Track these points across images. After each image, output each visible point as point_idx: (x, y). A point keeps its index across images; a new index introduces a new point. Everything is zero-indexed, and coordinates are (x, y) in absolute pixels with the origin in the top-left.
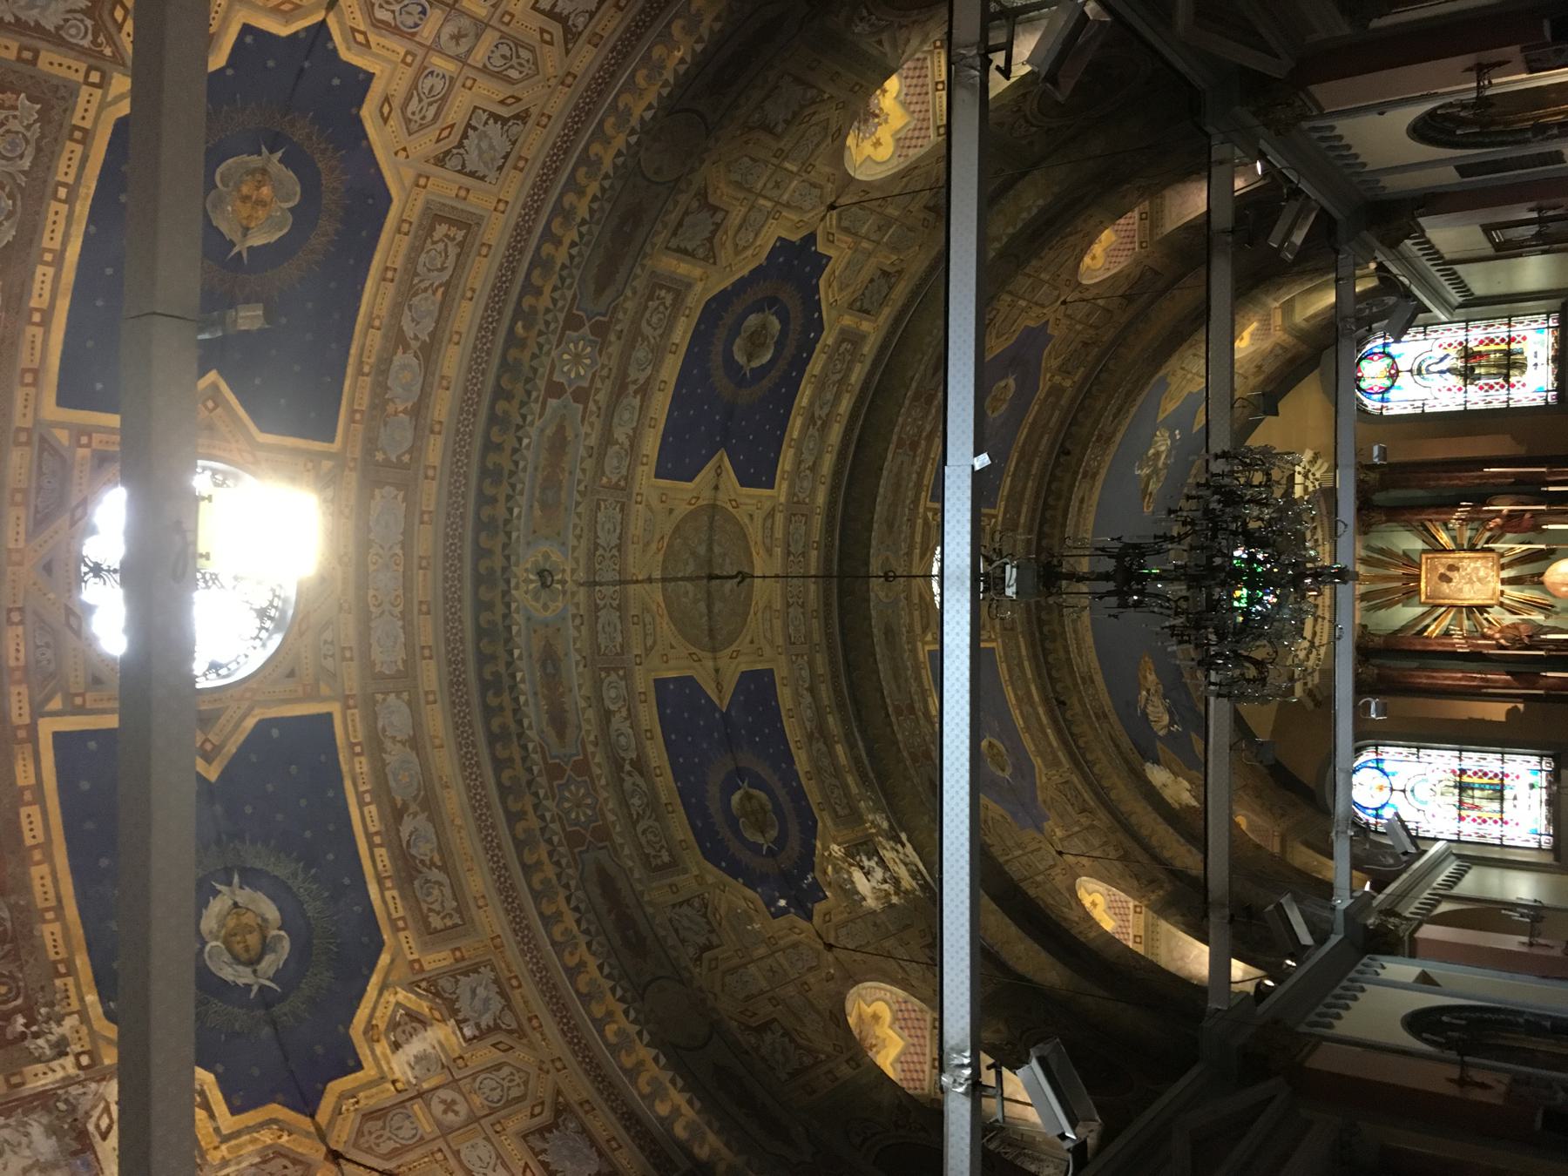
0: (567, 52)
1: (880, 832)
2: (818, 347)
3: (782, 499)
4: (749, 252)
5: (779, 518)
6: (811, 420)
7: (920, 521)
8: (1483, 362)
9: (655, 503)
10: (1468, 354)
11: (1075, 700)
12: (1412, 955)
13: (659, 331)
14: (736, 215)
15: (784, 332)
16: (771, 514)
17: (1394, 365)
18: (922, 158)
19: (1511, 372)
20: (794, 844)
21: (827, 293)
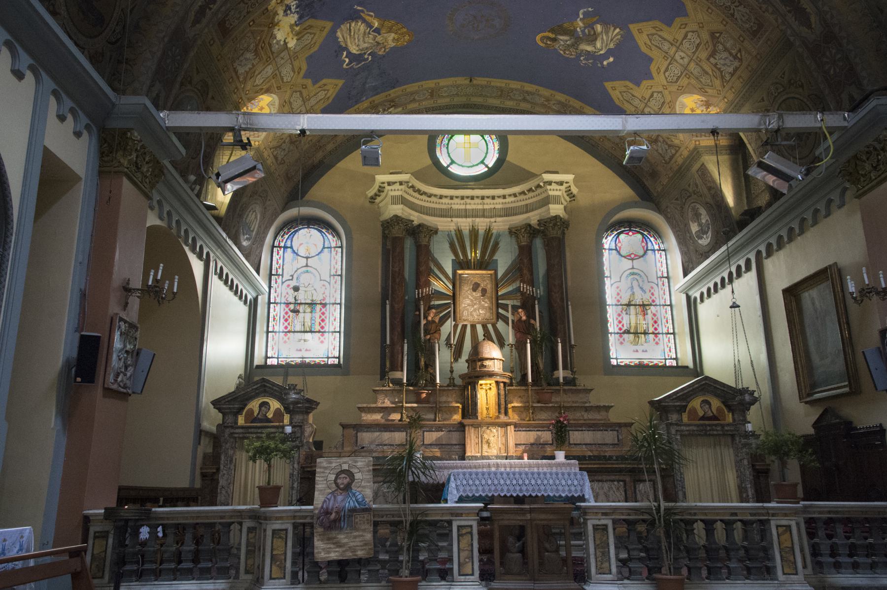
8: (641, 317)
12: (101, 173)
19: (631, 335)
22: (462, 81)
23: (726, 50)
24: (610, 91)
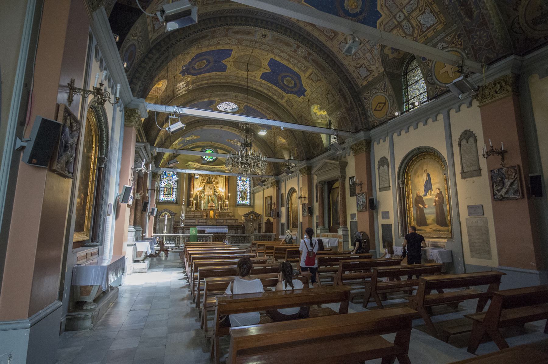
0: (354, 66)
1: (189, 88)
2: (284, 92)
3: (257, 79)
4: (306, 85)
5: (253, 78)
6: (270, 87)
7: (242, 102)
9: (266, 57)
10: (245, 192)
12: (152, 181)
13: (298, 66)
14: (314, 85)
15: (289, 87)
16: (255, 77)
17: (245, 181)
18: (312, 116)
20: (193, 71)
21: (293, 95)
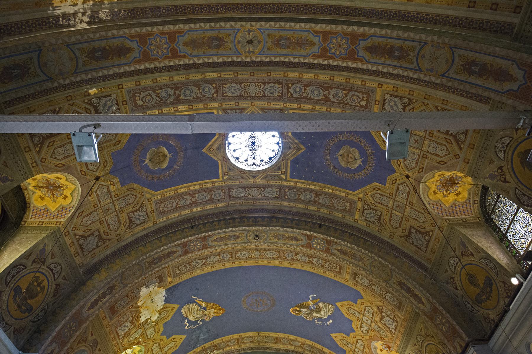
11: (193, 232)
22: (254, 334)
23: (388, 316)
24: (334, 338)
